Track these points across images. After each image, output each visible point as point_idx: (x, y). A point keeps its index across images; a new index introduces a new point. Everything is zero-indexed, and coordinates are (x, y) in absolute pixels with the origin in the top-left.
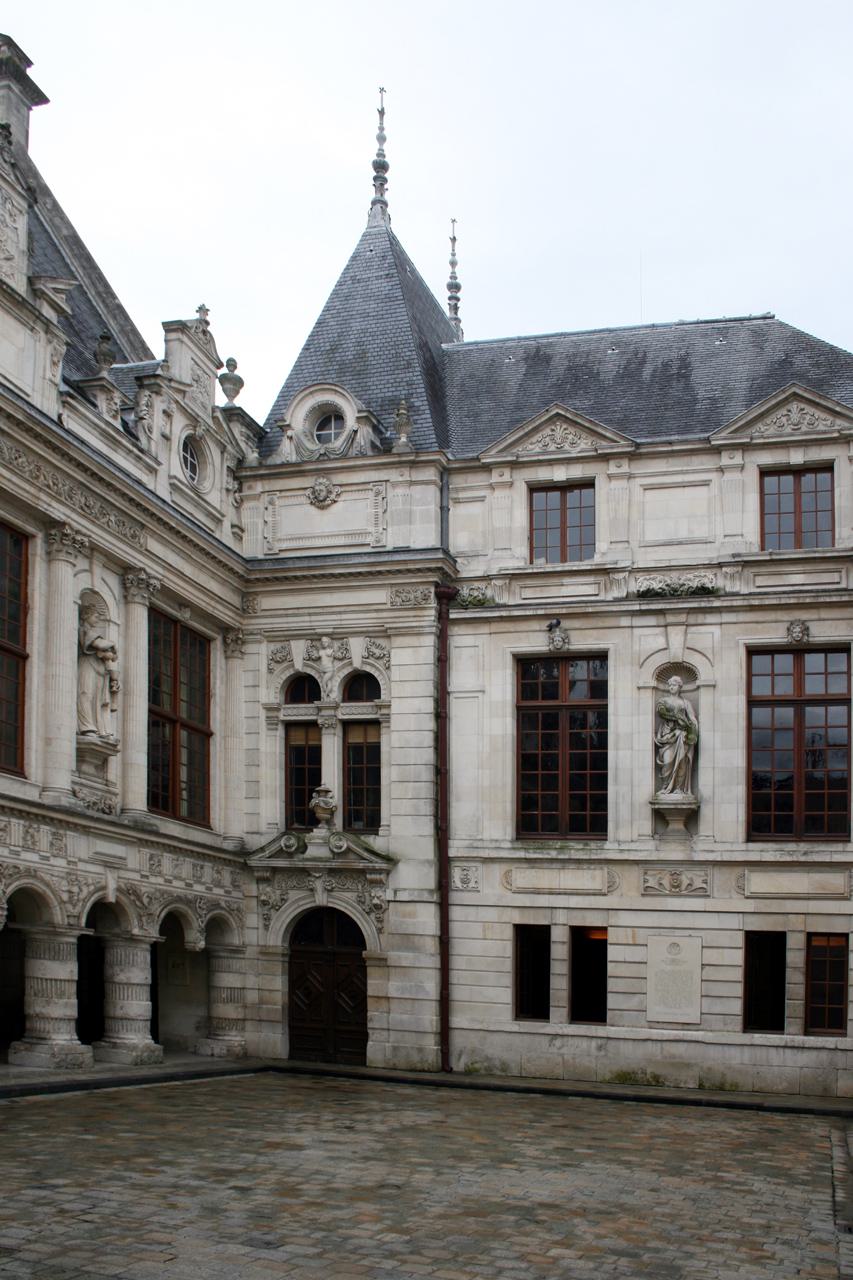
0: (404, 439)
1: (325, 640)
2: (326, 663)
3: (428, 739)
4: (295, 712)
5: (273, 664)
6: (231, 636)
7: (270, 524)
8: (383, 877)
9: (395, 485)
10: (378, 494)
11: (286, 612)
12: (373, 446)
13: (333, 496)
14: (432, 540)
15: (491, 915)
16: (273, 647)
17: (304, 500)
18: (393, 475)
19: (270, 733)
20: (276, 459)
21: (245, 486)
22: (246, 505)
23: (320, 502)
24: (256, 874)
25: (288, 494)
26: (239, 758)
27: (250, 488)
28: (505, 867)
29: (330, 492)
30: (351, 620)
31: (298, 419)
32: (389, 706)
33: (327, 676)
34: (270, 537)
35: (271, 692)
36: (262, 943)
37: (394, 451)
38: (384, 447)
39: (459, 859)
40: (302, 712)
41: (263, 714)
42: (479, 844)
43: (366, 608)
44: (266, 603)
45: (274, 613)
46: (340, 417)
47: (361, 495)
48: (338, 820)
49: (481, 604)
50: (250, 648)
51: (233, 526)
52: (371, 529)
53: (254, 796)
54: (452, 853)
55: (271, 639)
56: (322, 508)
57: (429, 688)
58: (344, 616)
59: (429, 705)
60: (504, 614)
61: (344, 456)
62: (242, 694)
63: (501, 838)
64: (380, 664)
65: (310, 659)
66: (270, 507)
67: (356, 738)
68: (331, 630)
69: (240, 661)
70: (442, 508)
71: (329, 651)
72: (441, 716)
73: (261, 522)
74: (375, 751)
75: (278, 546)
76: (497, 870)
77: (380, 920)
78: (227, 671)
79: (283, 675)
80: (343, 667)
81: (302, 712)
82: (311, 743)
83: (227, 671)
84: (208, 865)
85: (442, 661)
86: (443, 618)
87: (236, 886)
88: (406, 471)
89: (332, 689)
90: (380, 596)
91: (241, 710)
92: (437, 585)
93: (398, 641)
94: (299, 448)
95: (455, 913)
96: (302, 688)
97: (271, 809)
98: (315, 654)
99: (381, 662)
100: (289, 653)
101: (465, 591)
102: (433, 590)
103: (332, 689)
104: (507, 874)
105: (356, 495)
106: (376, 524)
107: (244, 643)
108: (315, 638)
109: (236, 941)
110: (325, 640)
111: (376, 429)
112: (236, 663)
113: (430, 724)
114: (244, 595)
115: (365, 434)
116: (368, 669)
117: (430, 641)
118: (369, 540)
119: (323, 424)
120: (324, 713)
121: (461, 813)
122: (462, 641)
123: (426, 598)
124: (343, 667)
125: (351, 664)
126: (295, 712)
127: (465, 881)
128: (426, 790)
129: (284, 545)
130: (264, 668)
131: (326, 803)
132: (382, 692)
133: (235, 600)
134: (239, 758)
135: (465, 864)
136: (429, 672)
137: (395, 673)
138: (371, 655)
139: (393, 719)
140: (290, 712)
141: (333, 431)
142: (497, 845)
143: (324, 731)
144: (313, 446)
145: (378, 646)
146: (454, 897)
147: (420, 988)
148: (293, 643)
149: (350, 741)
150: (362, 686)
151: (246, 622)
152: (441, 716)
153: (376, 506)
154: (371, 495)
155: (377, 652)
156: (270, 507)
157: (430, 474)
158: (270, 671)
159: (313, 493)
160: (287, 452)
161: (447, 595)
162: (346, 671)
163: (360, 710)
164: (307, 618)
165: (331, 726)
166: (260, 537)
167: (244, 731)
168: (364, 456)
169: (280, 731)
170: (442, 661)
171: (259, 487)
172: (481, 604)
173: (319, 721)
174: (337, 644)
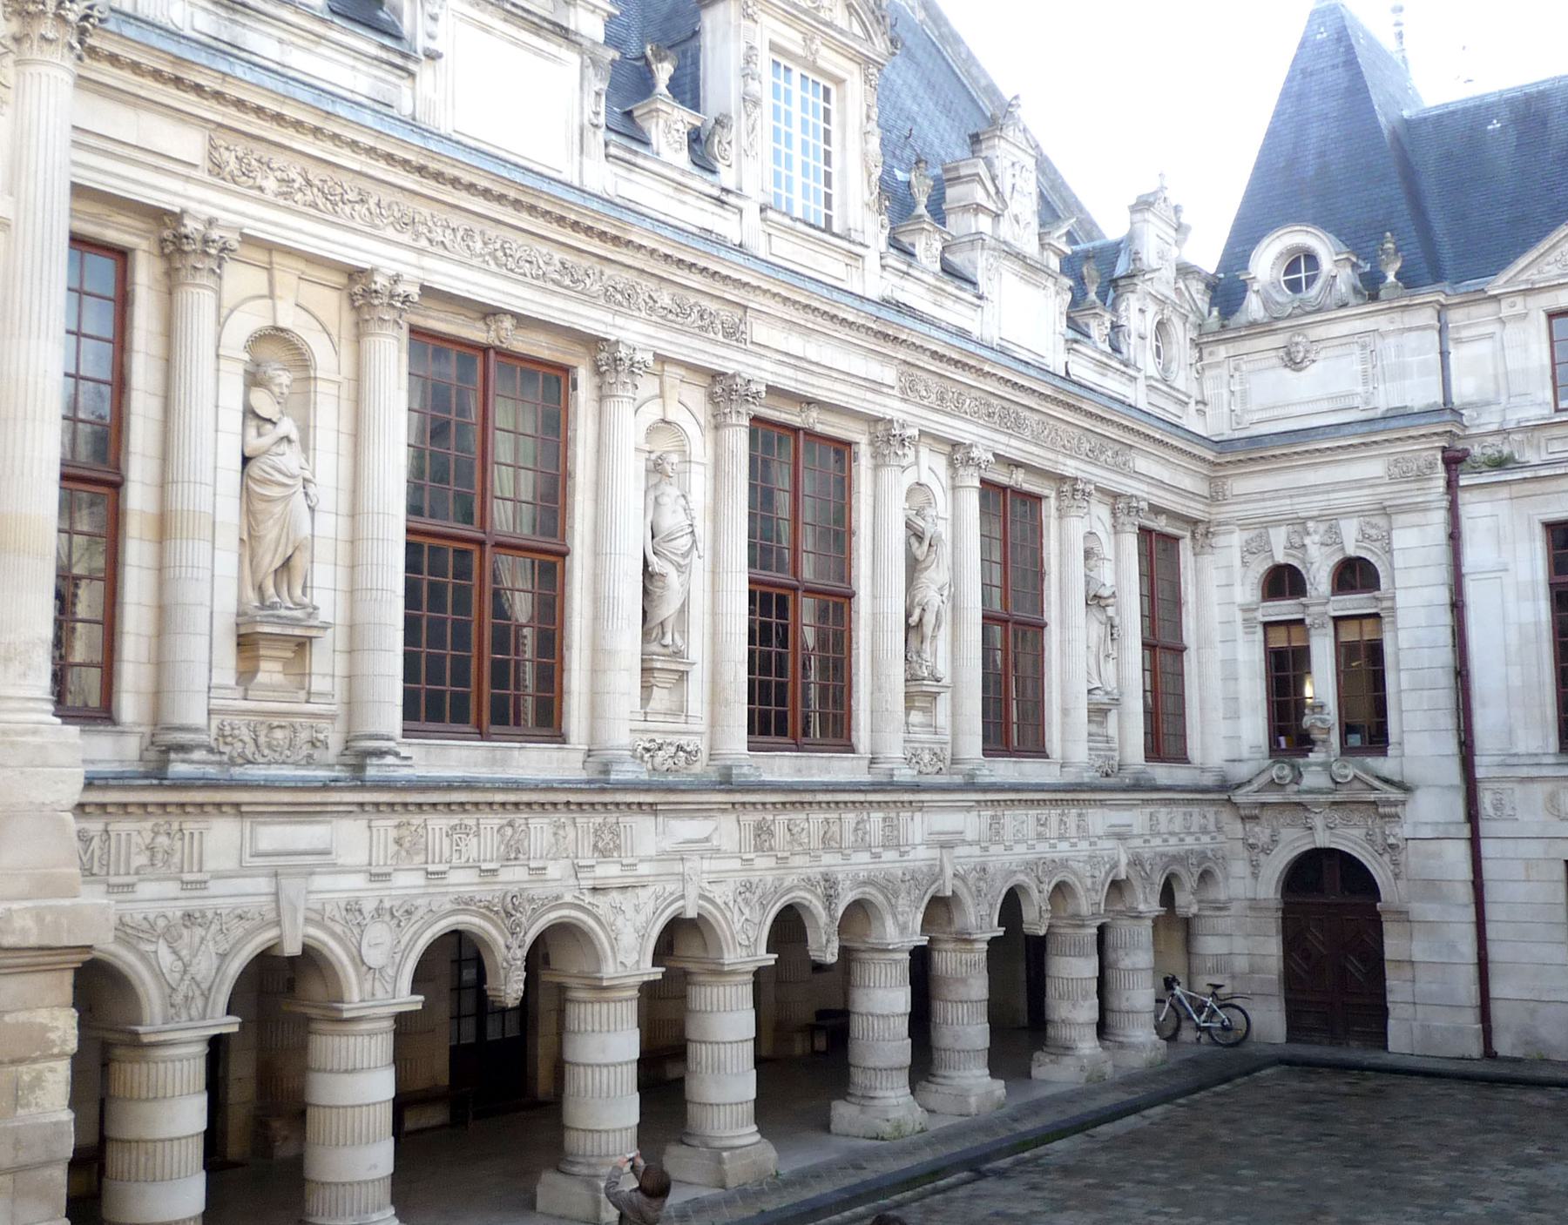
0: (1391, 278)
1: (1310, 524)
2: (1314, 551)
3: (1445, 636)
4: (1276, 610)
5: (1248, 558)
6: (1201, 529)
7: (1238, 394)
8: (1399, 809)
9: (1383, 335)
10: (1364, 347)
11: (1263, 496)
12: (1355, 290)
13: (1312, 356)
14: (1437, 398)
15: (1535, 849)
16: (1247, 535)
17: (1275, 361)
18: (1381, 322)
19: (1251, 637)
20: (1240, 318)
21: (1205, 352)
22: (1208, 373)
23: (1293, 362)
24: (1242, 812)
25: (1257, 356)
26: (1215, 672)
27: (1211, 354)
28: (1548, 787)
29: (1307, 351)
30: (1342, 499)
31: (1265, 264)
32: (1393, 598)
33: (1315, 566)
34: (1238, 409)
35: (1247, 590)
36: (1251, 895)
37: (1382, 293)
38: (1370, 287)
39: (1489, 779)
40: (1284, 609)
41: (1239, 616)
42: (1515, 760)
43: (1359, 484)
44: (1241, 485)
45: (1248, 498)
46: (1311, 259)
47: (1345, 350)
48: (1335, 739)
49: (1500, 463)
50: (1219, 541)
51: (1197, 403)
52: (1360, 389)
53: (1234, 716)
54: (1480, 773)
55: (1243, 527)
56: (1300, 370)
57: (1440, 574)
58: (1333, 496)
59: (1443, 596)
60: (1528, 475)
61: (1319, 311)
62: (1214, 595)
63: (1540, 751)
64: (1376, 546)
65: (1292, 547)
66: (1237, 375)
67: (1350, 634)
68: (1315, 513)
69: (1210, 558)
70: (1441, 353)
71: (1316, 538)
72: (1457, 606)
73: (1226, 395)
74: (1375, 651)
75: (1247, 418)
76: (1539, 791)
77: (1395, 863)
78: (1198, 571)
79: (1260, 567)
80: (1333, 554)
81: (1284, 610)
82: (1294, 644)
83: (1198, 571)
84: (1195, 810)
85: (1455, 537)
86: (1452, 486)
87: (1219, 829)
88: (1396, 316)
89: (1320, 578)
90: (1372, 468)
91: (1215, 613)
92: (1444, 449)
93: (1399, 520)
94: (1267, 303)
95: (1487, 848)
96: (1283, 582)
97: (1254, 727)
98: (1296, 540)
99: (1378, 544)
100: (1268, 542)
101: (1476, 450)
102: (1439, 456)
103: (1320, 578)
104: (1552, 799)
105: (1339, 351)
106: (1365, 383)
107: (1213, 534)
108: (1300, 524)
109: (1222, 897)
110: (1310, 524)
111: (1354, 266)
112: (1207, 559)
113: (1446, 618)
114: (1211, 480)
115: (1345, 279)
116: (1363, 554)
117: (1439, 517)
118: (1357, 402)
119: (1292, 267)
120: (1312, 610)
121: (1485, 721)
122: (1479, 512)
123: (1431, 466)
124: (1333, 554)
125: (1343, 549)
126: (1276, 610)
127: (1498, 806)
128: (1445, 698)
129: (1256, 417)
130: (1237, 562)
131: (1323, 721)
132: (1382, 581)
133: (1202, 488)
134: (1215, 672)
135: (1497, 785)
136: (1441, 553)
137: (1399, 561)
138: (1366, 536)
139: (1399, 613)
140: (1270, 611)
141: (1303, 275)
142: (1536, 760)
143: (1313, 632)
144: (1284, 296)
145: (1374, 526)
146: (1485, 828)
147: (1452, 947)
148: (1271, 531)
149: (1344, 638)
150: (1355, 574)
151: (1214, 510)
152: (1457, 606)
153: (1364, 361)
154: (1356, 348)
155: (1373, 532)
156: (1237, 375)
157: (1427, 316)
158: (1244, 564)
159: (1288, 354)
160: (1253, 307)
161: (1454, 461)
162: (1338, 557)
163: (1354, 603)
164: (1288, 501)
165: (1323, 626)
166: (1226, 410)
167: (1218, 638)
168: (1344, 305)
169: (1260, 630)
170: (1455, 537)
171: (1222, 351)
172: (1500, 463)
173: (1308, 621)
174: (1322, 527)
